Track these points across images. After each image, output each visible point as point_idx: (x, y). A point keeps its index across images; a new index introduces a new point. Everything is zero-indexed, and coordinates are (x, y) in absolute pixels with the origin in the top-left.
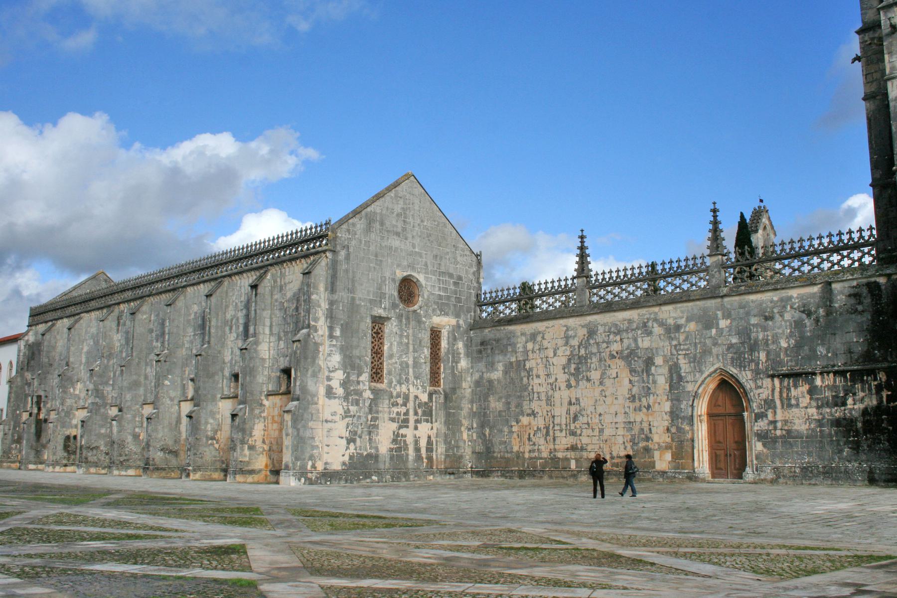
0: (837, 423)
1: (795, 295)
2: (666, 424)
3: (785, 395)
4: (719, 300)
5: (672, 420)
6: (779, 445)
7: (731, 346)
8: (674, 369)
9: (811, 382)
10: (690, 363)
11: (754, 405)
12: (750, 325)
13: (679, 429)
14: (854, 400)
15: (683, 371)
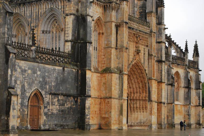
0: (62, 111)
1: (57, 69)
2: (19, 108)
3: (52, 101)
4: (38, 64)
5: (21, 107)
6: (50, 117)
7: (40, 82)
8: (23, 86)
9: (58, 98)
10: (28, 85)
11: (45, 103)
12: (45, 75)
13: (23, 110)
14: (66, 104)
15: (25, 88)
